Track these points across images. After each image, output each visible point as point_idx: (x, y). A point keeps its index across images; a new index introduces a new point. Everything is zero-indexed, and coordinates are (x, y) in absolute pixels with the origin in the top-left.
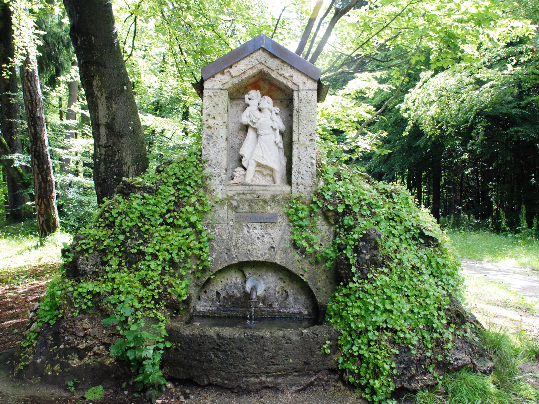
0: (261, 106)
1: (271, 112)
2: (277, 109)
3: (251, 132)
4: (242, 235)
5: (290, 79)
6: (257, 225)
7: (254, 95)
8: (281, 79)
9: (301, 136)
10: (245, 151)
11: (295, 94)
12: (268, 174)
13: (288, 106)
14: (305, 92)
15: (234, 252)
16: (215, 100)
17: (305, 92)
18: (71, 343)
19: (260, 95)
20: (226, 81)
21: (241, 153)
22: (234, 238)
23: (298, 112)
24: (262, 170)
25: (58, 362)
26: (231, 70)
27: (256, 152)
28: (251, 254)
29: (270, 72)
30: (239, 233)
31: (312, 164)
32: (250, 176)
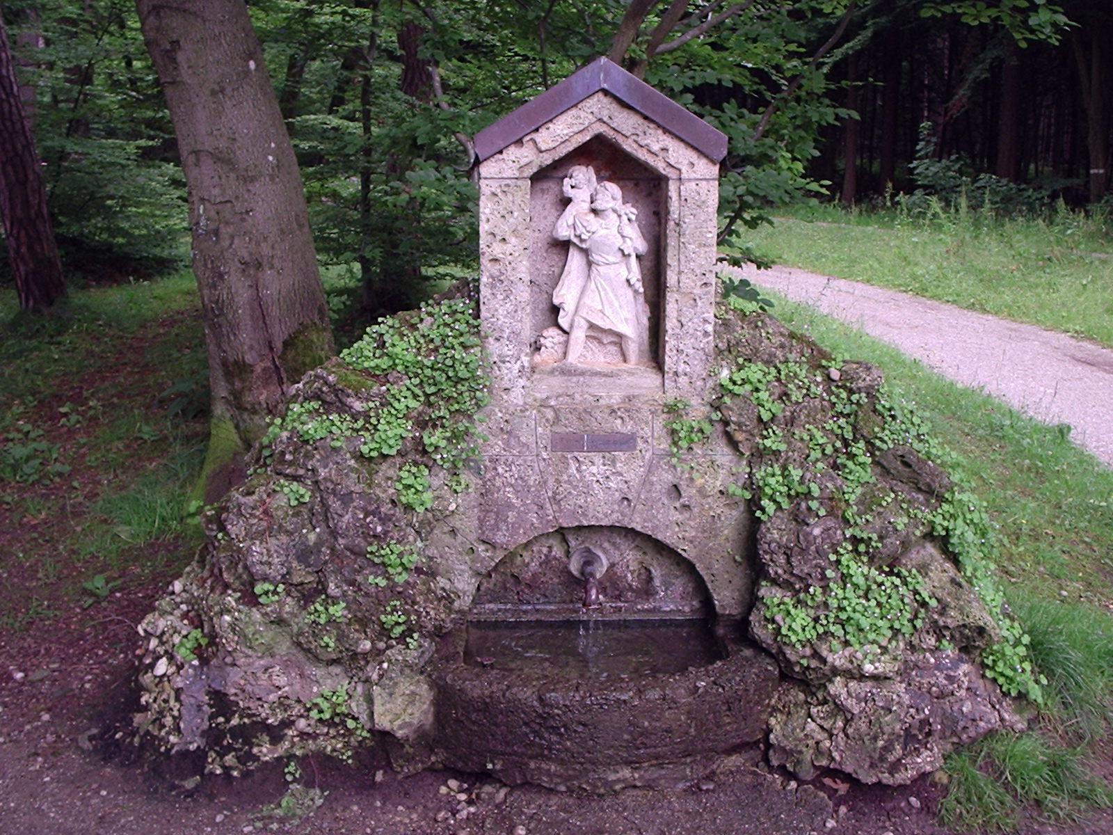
0: (598, 205)
1: (620, 216)
2: (631, 211)
3: (575, 260)
4: (565, 477)
5: (661, 154)
6: (597, 458)
7: (582, 180)
8: (642, 155)
9: (683, 277)
10: (566, 295)
11: (672, 187)
12: (611, 343)
13: (650, 194)
14: (693, 184)
15: (550, 509)
16: (506, 200)
17: (693, 184)
18: (254, 715)
19: (594, 178)
20: (526, 160)
21: (556, 301)
22: (551, 483)
23: (678, 225)
24: (599, 335)
25: (230, 748)
26: (538, 137)
27: (587, 300)
28: (584, 514)
29: (620, 139)
30: (561, 473)
31: (706, 334)
32: (580, 352)
